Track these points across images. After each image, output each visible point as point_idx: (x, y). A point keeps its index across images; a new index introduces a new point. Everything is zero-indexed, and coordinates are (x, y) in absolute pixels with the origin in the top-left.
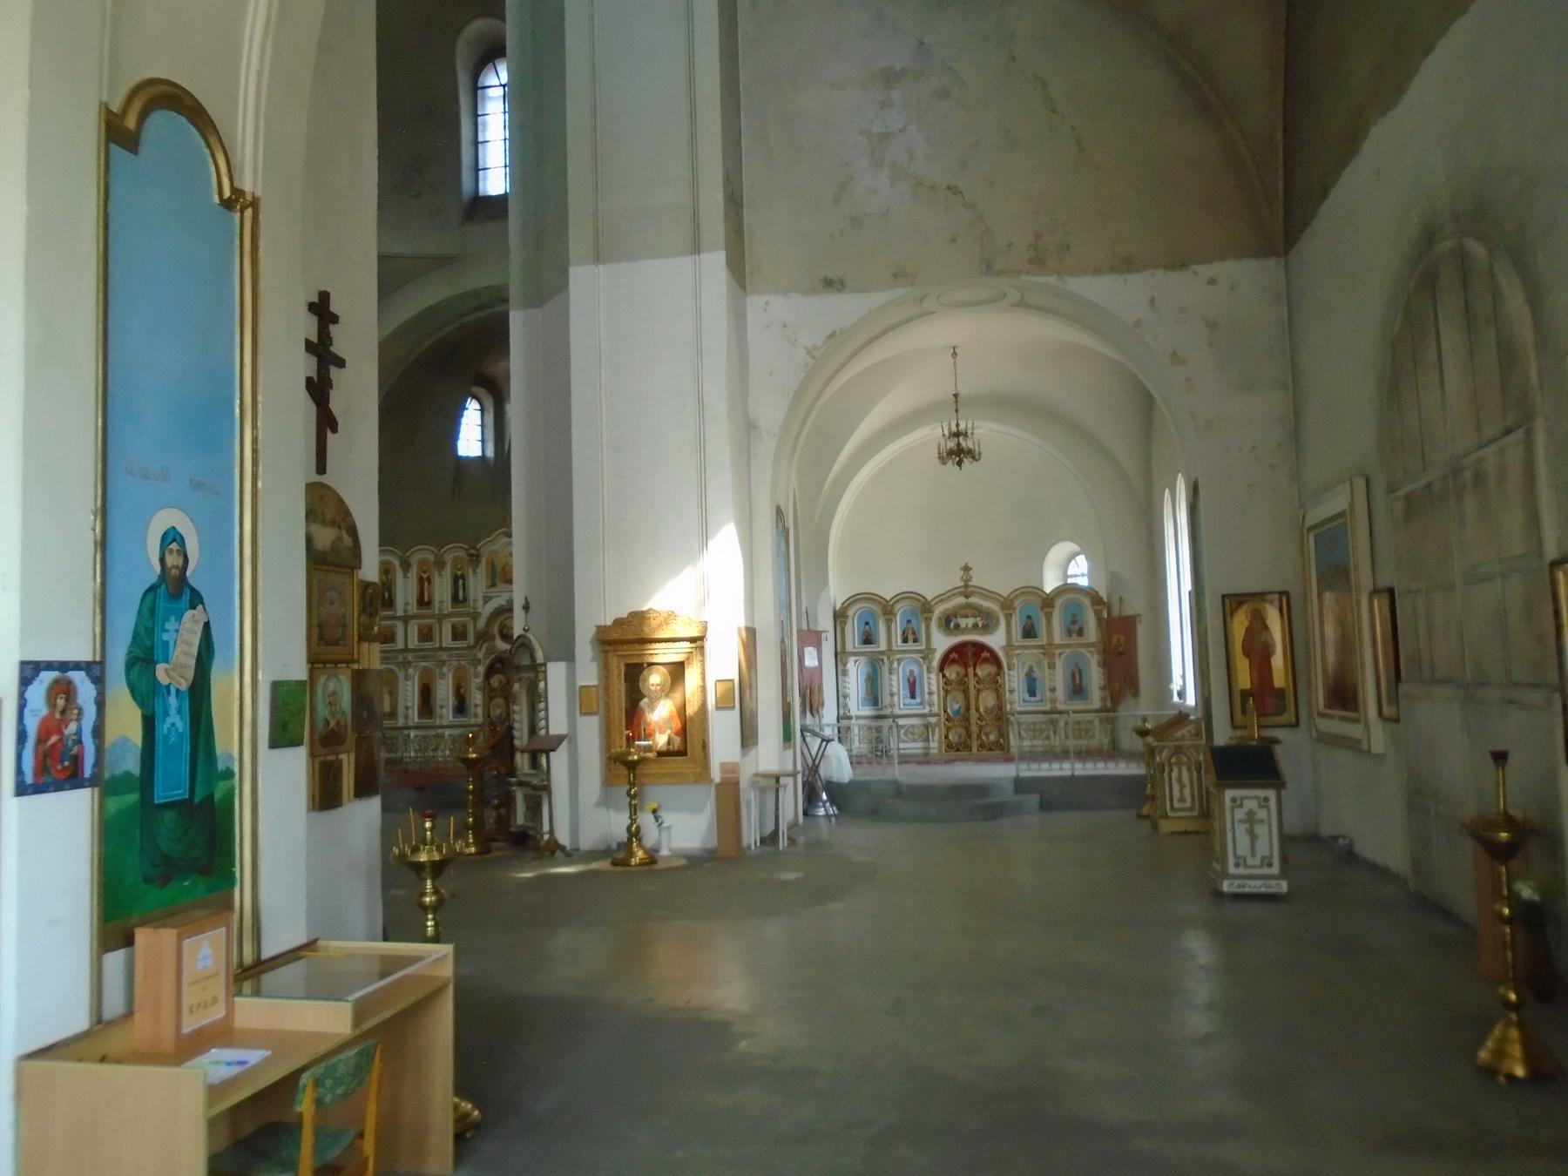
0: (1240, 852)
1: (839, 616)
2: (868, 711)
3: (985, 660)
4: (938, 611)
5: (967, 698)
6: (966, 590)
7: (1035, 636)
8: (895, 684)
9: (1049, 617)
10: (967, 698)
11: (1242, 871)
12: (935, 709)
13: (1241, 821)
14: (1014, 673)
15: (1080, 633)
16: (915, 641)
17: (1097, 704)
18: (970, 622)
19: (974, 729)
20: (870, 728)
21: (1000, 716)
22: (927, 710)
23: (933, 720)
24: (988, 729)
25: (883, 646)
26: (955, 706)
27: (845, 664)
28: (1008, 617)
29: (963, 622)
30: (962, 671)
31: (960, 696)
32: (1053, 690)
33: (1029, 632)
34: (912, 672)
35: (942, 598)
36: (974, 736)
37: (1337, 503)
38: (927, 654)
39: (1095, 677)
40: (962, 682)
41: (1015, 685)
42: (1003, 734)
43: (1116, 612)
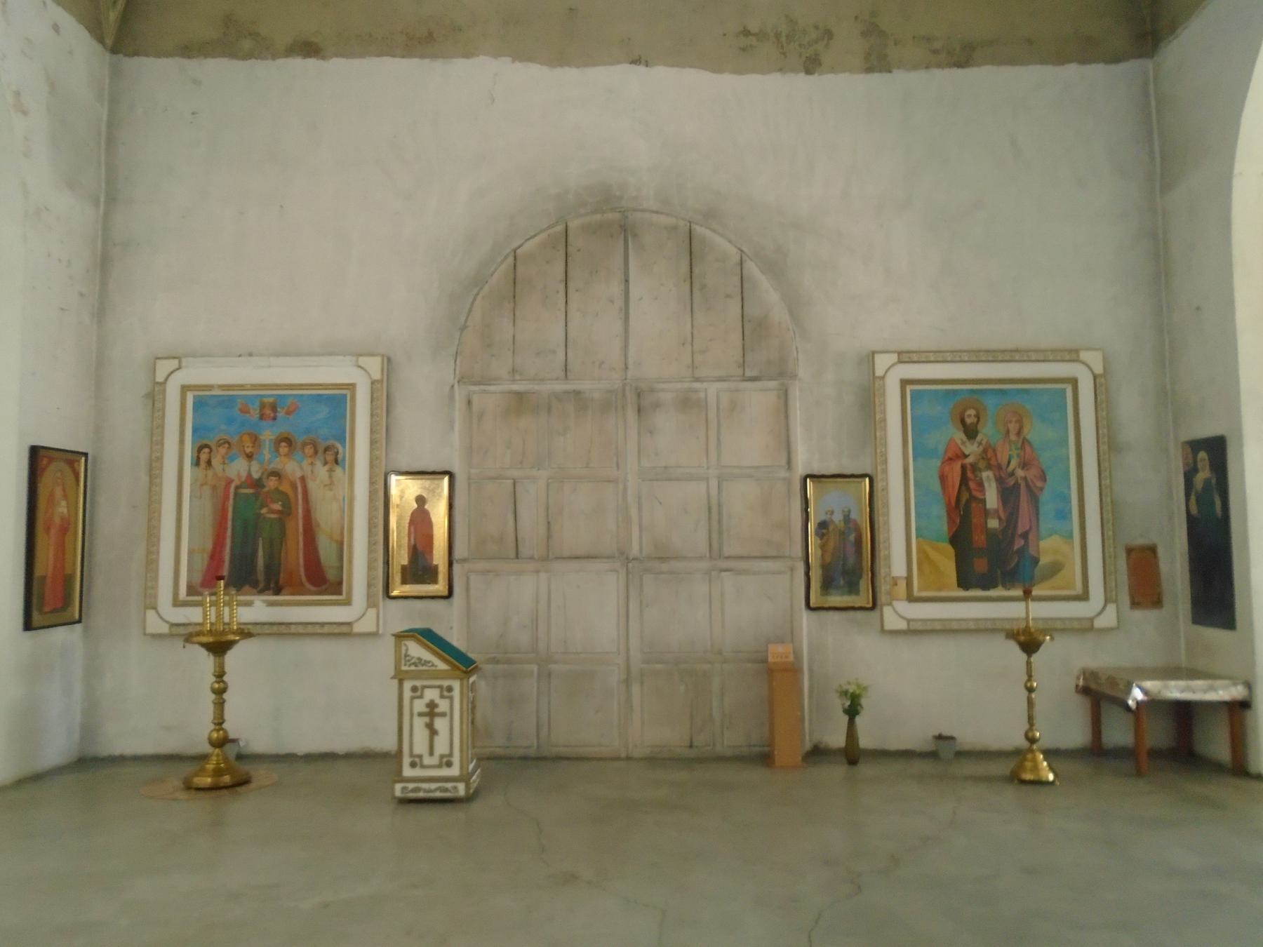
0: (417, 751)
11: (417, 772)
13: (420, 714)
37: (356, 375)
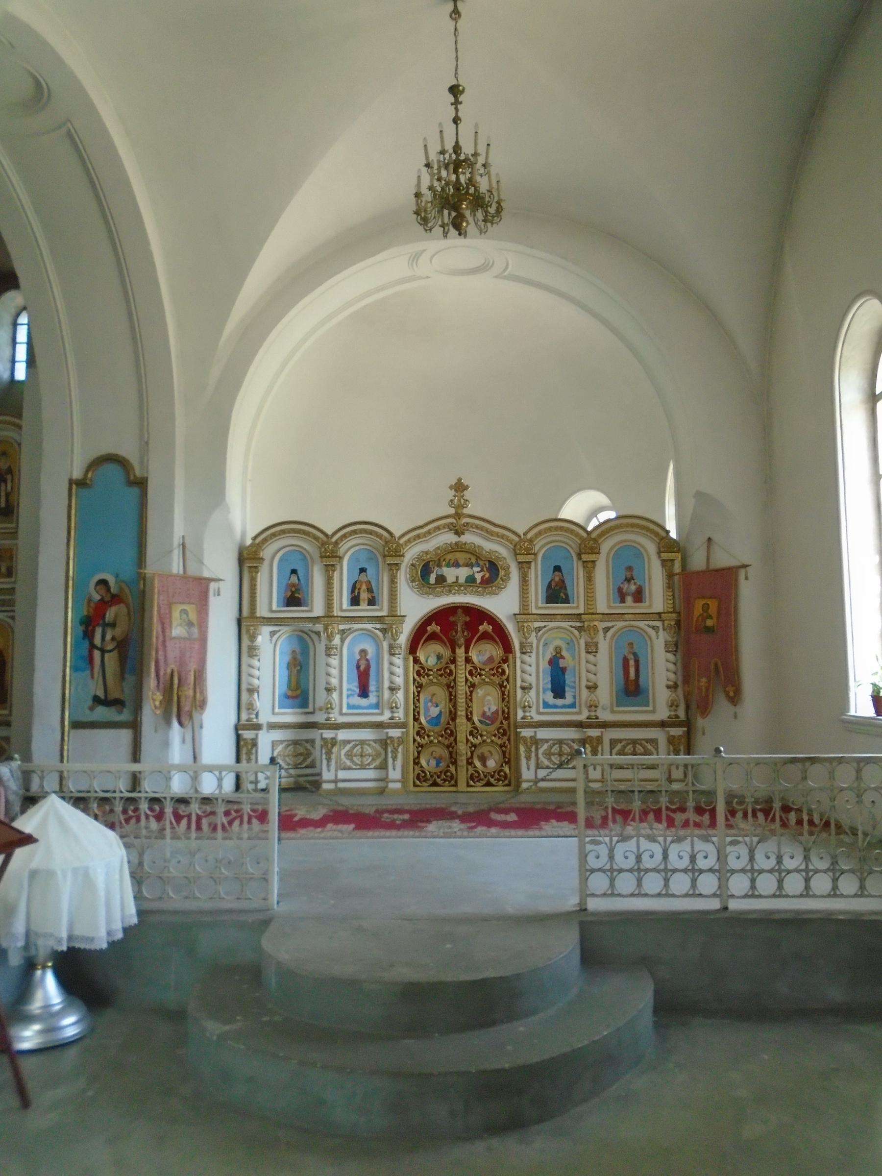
1: (248, 559)
2: (290, 716)
3: (485, 636)
4: (411, 553)
5: (452, 699)
6: (458, 522)
7: (566, 601)
8: (336, 672)
9: (589, 567)
10: (452, 699)
12: (400, 715)
14: (531, 659)
15: (638, 596)
16: (372, 602)
17: (663, 713)
18: (463, 573)
19: (463, 748)
20: (296, 743)
21: (505, 725)
22: (385, 717)
23: (395, 733)
24: (484, 750)
25: (318, 609)
26: (433, 708)
27: (253, 638)
28: (524, 567)
29: (451, 574)
30: (446, 653)
31: (441, 694)
32: (592, 688)
33: (556, 593)
34: (363, 652)
35: (418, 533)
36: (462, 761)
38: (388, 624)
39: (661, 669)
40: (446, 671)
41: (532, 680)
42: (509, 758)
43: (698, 562)
